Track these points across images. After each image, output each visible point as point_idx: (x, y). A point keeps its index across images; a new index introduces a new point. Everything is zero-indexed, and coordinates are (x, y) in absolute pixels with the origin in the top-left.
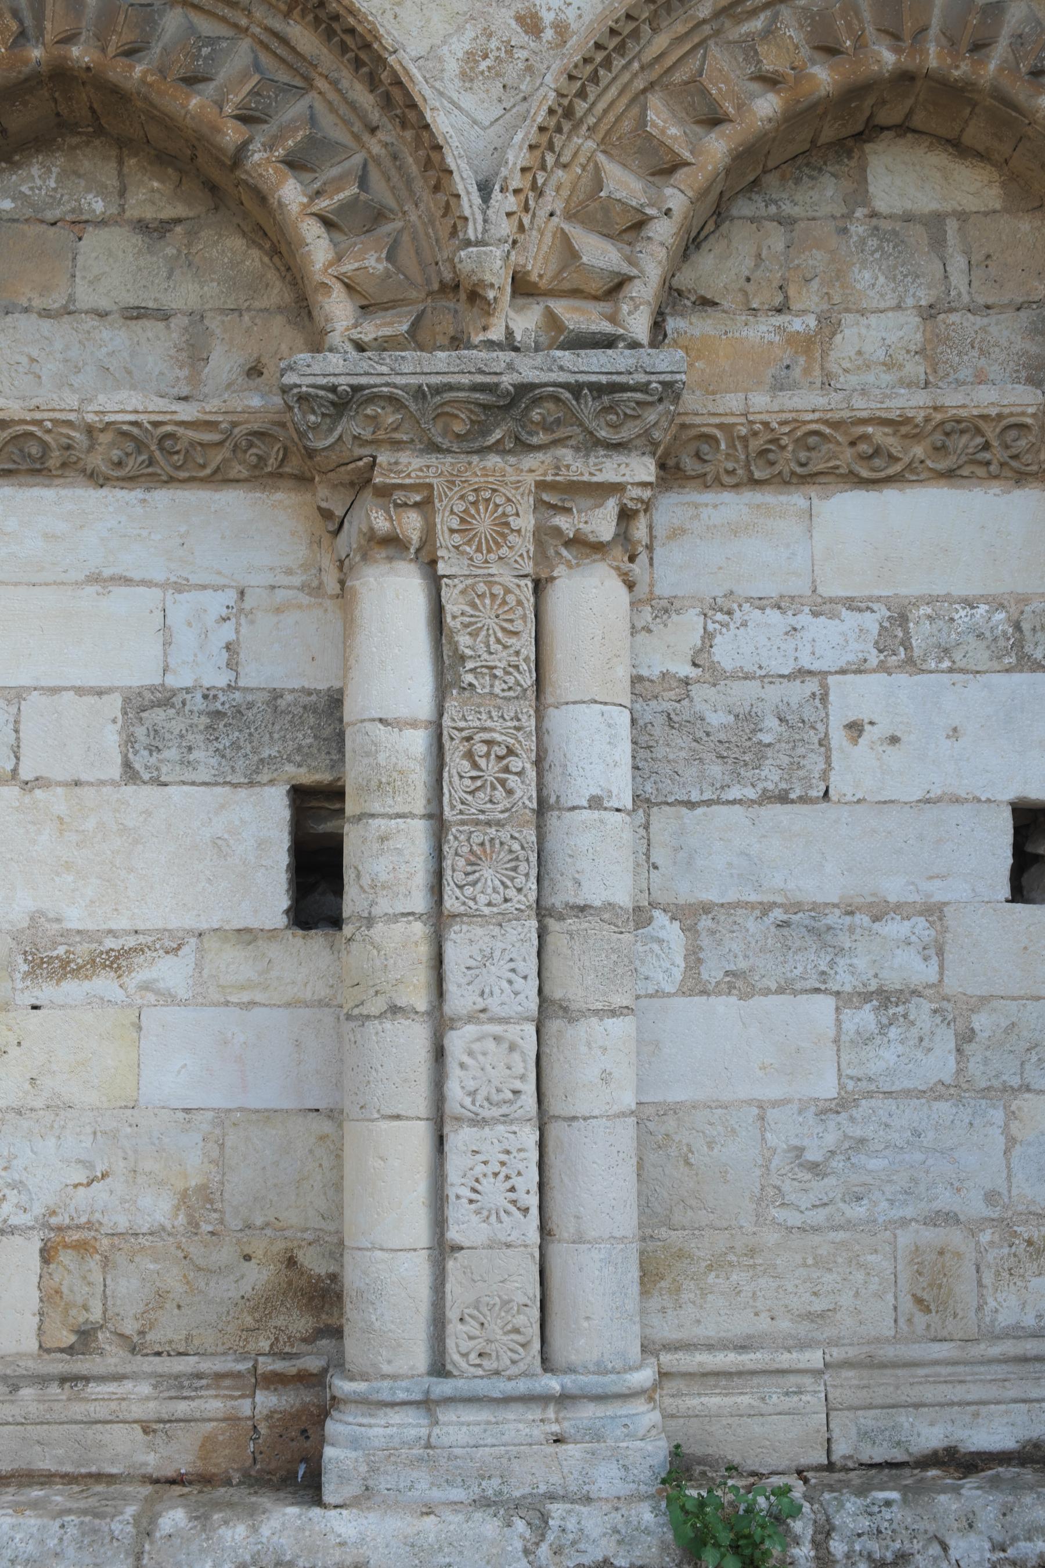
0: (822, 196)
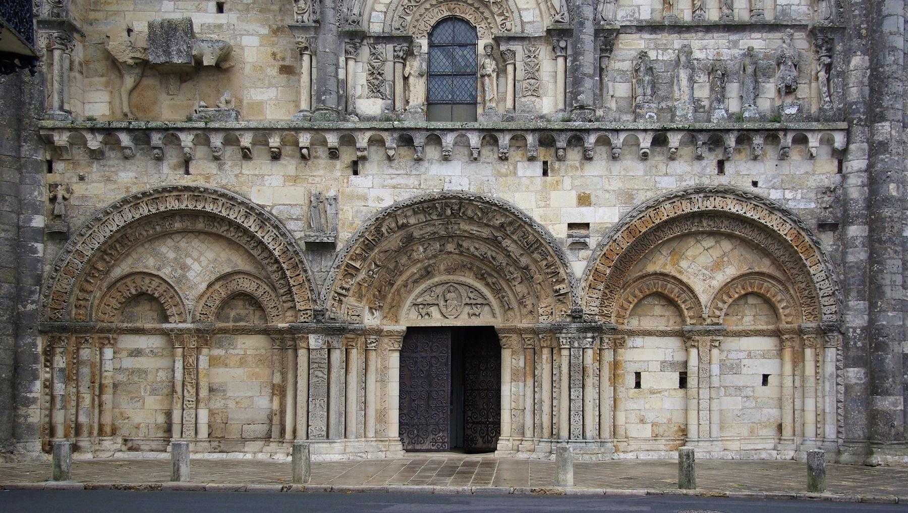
0: (742, 302)
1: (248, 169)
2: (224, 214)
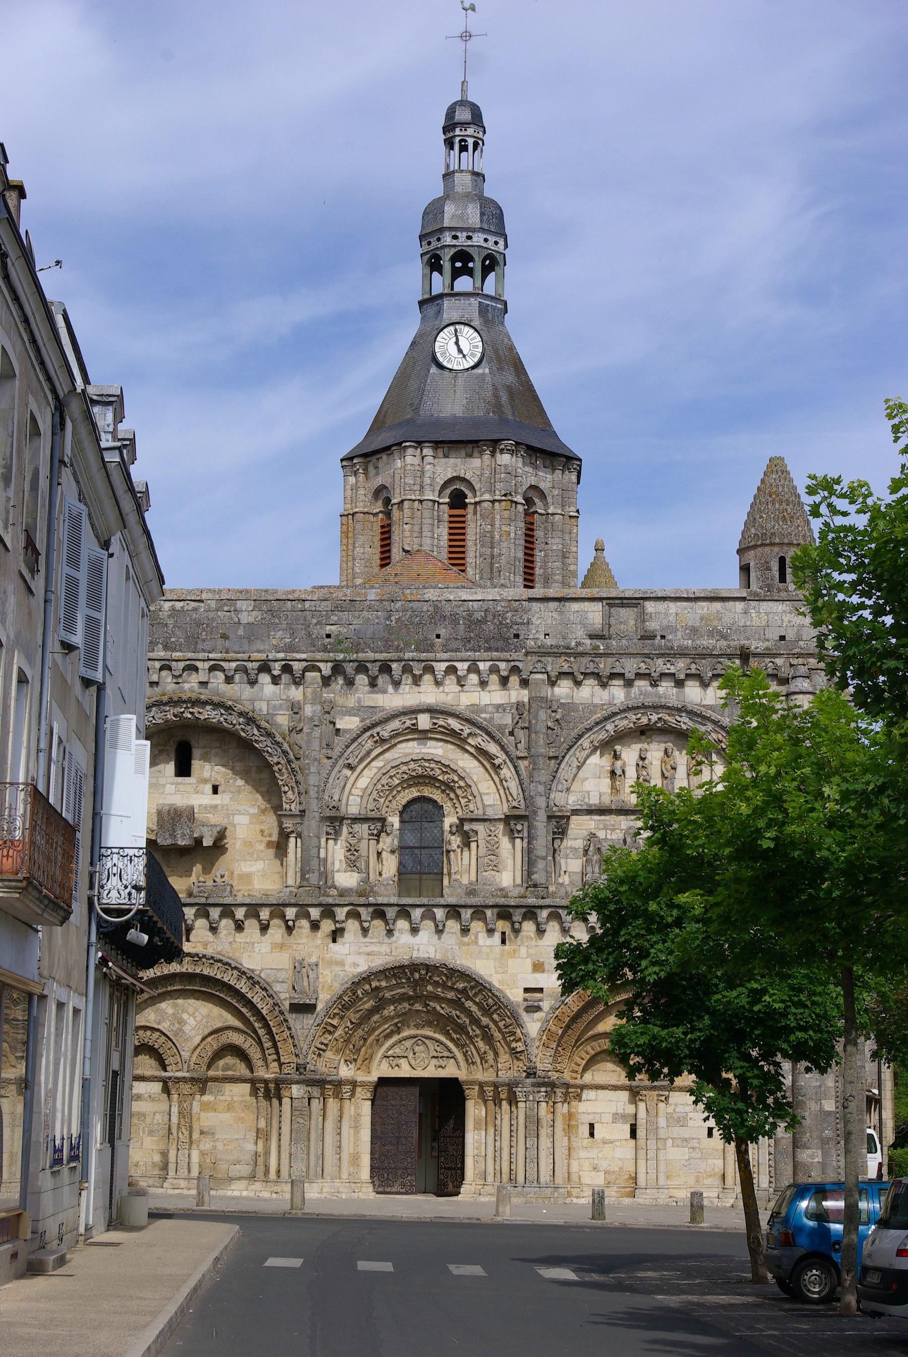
1: (240, 938)
2: (219, 977)
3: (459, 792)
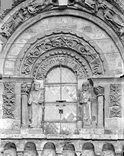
3: (88, 58)
